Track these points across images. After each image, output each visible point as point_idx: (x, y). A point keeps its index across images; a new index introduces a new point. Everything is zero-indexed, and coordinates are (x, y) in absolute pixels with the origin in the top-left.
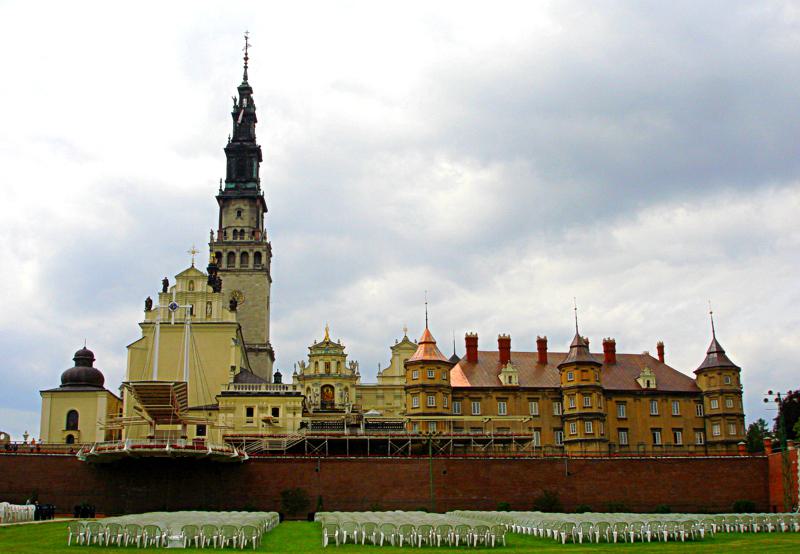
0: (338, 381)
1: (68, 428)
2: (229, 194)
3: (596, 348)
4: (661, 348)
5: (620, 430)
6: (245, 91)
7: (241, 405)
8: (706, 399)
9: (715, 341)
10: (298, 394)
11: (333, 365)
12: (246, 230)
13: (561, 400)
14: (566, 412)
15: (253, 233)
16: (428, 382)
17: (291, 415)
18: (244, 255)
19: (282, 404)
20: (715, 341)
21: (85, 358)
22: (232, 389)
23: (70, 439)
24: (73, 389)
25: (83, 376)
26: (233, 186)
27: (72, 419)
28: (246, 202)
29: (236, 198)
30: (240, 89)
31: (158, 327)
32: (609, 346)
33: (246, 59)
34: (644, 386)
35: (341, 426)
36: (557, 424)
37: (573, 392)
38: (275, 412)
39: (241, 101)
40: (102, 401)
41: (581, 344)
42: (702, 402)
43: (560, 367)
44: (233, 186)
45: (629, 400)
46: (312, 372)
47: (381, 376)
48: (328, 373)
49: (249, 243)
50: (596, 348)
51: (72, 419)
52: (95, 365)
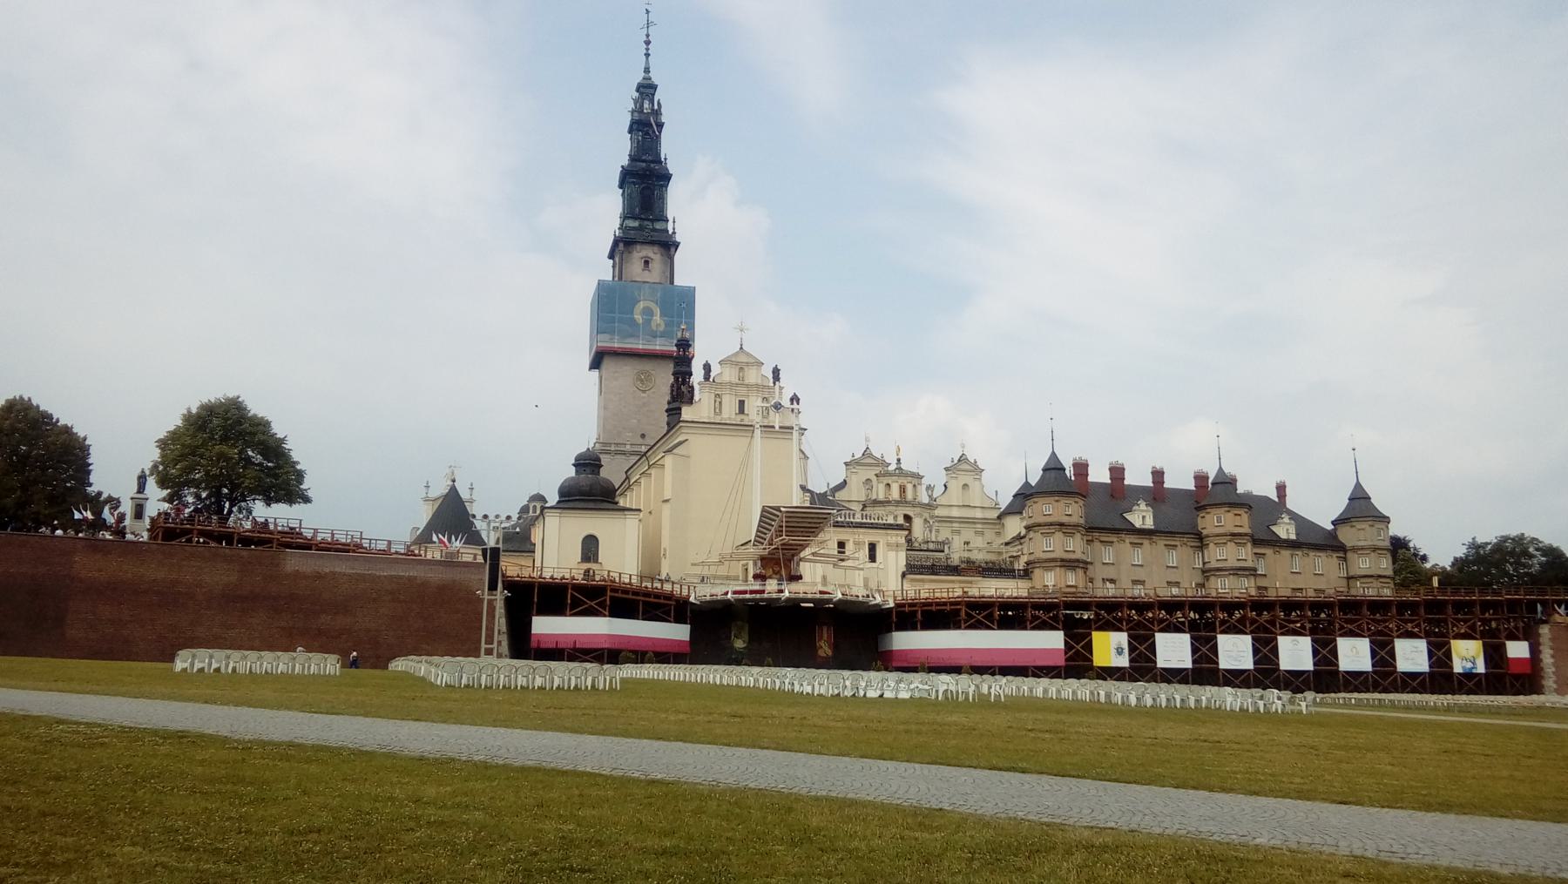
0: (918, 510)
4: (1281, 489)
5: (1259, 588)
6: (647, 89)
8: (1349, 555)
9: (1358, 486)
10: (899, 527)
11: (909, 488)
14: (1214, 565)
16: (1065, 520)
20: (1358, 486)
24: (591, 505)
26: (636, 224)
27: (590, 547)
28: (656, 249)
31: (758, 432)
33: (648, 43)
34: (1283, 536)
36: (1200, 580)
42: (1345, 559)
44: (636, 224)
45: (1268, 551)
46: (881, 497)
48: (902, 501)
51: (590, 547)
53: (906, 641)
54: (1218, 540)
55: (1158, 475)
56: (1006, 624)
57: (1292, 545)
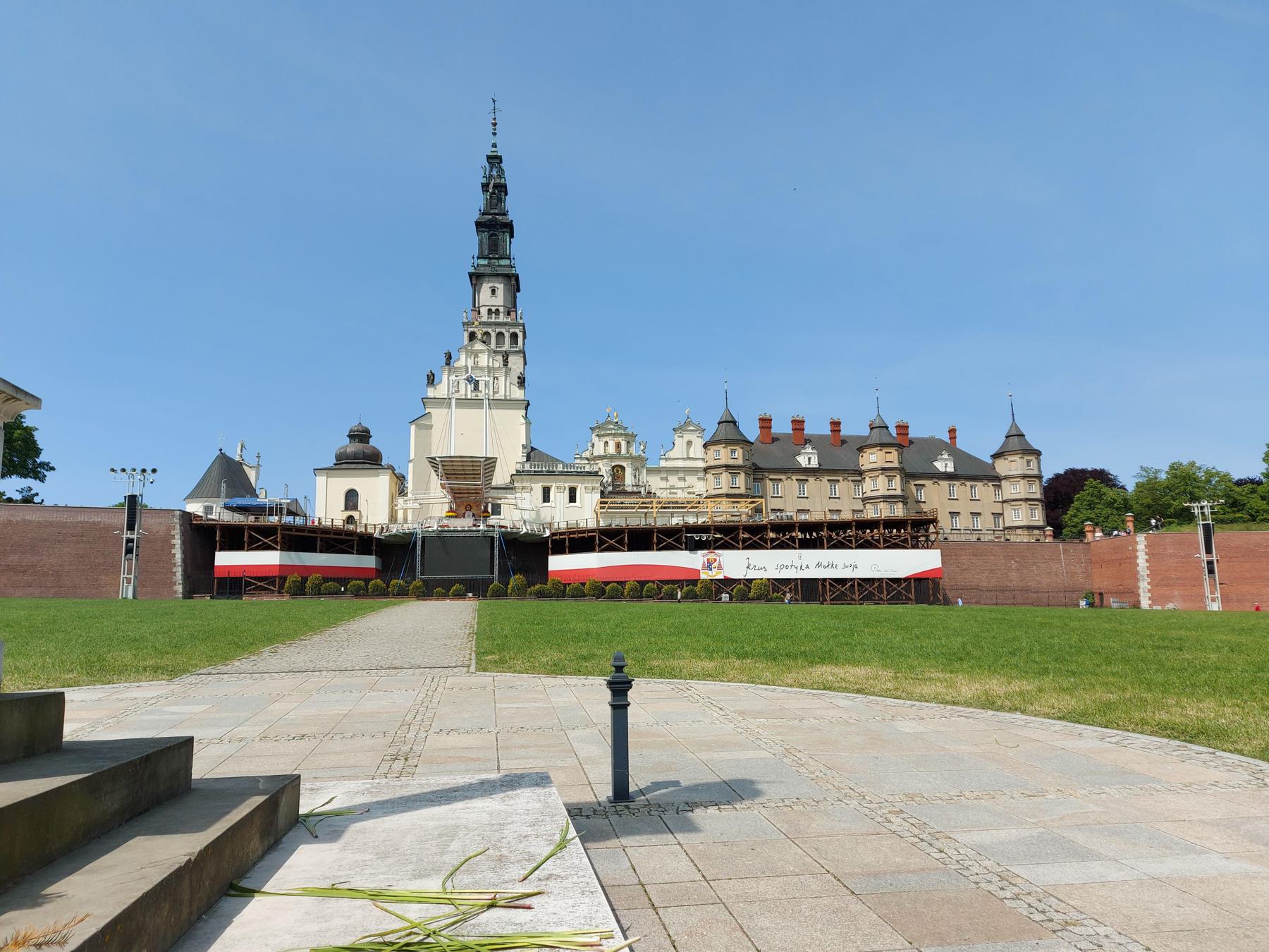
1: (347, 508)
2: (482, 270)
4: (952, 431)
6: (495, 160)
8: (1003, 483)
11: (623, 444)
12: (501, 309)
14: (869, 494)
16: (731, 462)
20: (1014, 424)
22: (527, 467)
26: (485, 262)
27: (351, 498)
28: (500, 279)
29: (490, 275)
30: (489, 158)
32: (903, 429)
33: (495, 124)
37: (876, 473)
39: (491, 170)
42: (999, 486)
46: (602, 453)
49: (505, 324)
51: (351, 498)
52: (372, 442)
53: (557, 563)
55: (836, 425)
56: (633, 547)
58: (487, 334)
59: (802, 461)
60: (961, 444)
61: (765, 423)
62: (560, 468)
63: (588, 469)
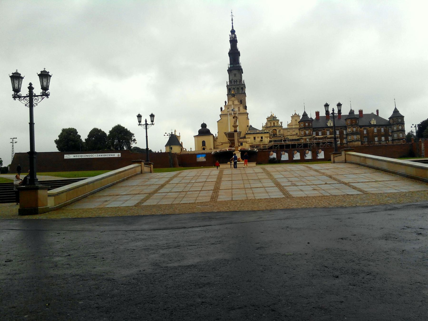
1: (203, 146)
3: (357, 113)
4: (377, 111)
6: (233, 32)
7: (252, 137)
9: (396, 109)
10: (268, 133)
11: (276, 123)
13: (346, 129)
15: (240, 81)
17: (266, 139)
18: (238, 88)
19: (264, 136)
20: (396, 109)
21: (204, 126)
22: (249, 132)
23: (204, 149)
25: (204, 131)
26: (232, 66)
27: (204, 143)
28: (237, 71)
32: (361, 112)
33: (232, 20)
34: (372, 124)
35: (281, 141)
38: (262, 138)
40: (211, 138)
41: (352, 112)
43: (345, 120)
44: (232, 66)
47: (288, 125)
50: (357, 113)
51: (204, 143)
52: (207, 128)
54: (349, 127)
57: (375, 126)
58: (234, 88)
59: (329, 125)
60: (380, 115)
61: (317, 113)
62: (258, 132)
63: (266, 131)
